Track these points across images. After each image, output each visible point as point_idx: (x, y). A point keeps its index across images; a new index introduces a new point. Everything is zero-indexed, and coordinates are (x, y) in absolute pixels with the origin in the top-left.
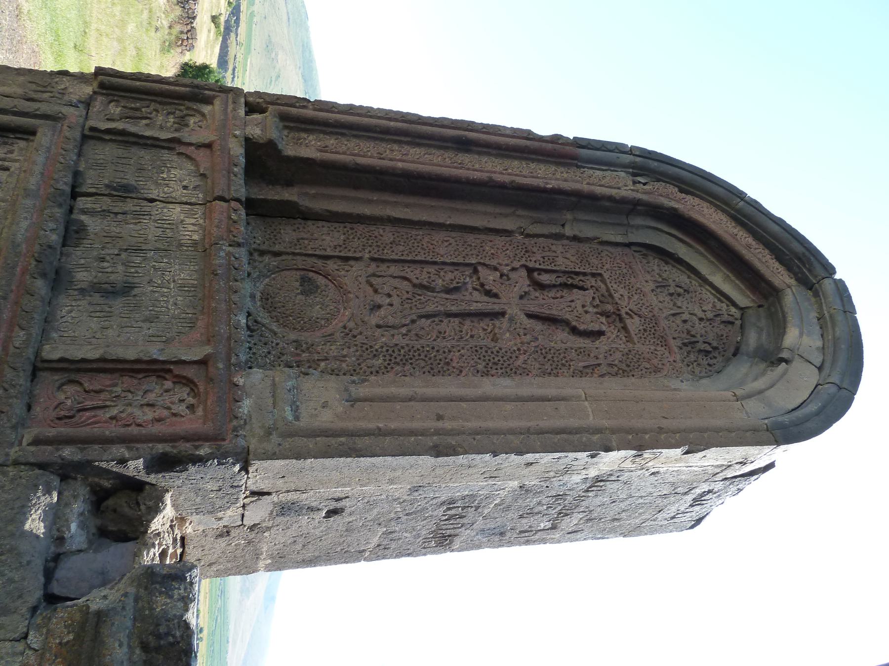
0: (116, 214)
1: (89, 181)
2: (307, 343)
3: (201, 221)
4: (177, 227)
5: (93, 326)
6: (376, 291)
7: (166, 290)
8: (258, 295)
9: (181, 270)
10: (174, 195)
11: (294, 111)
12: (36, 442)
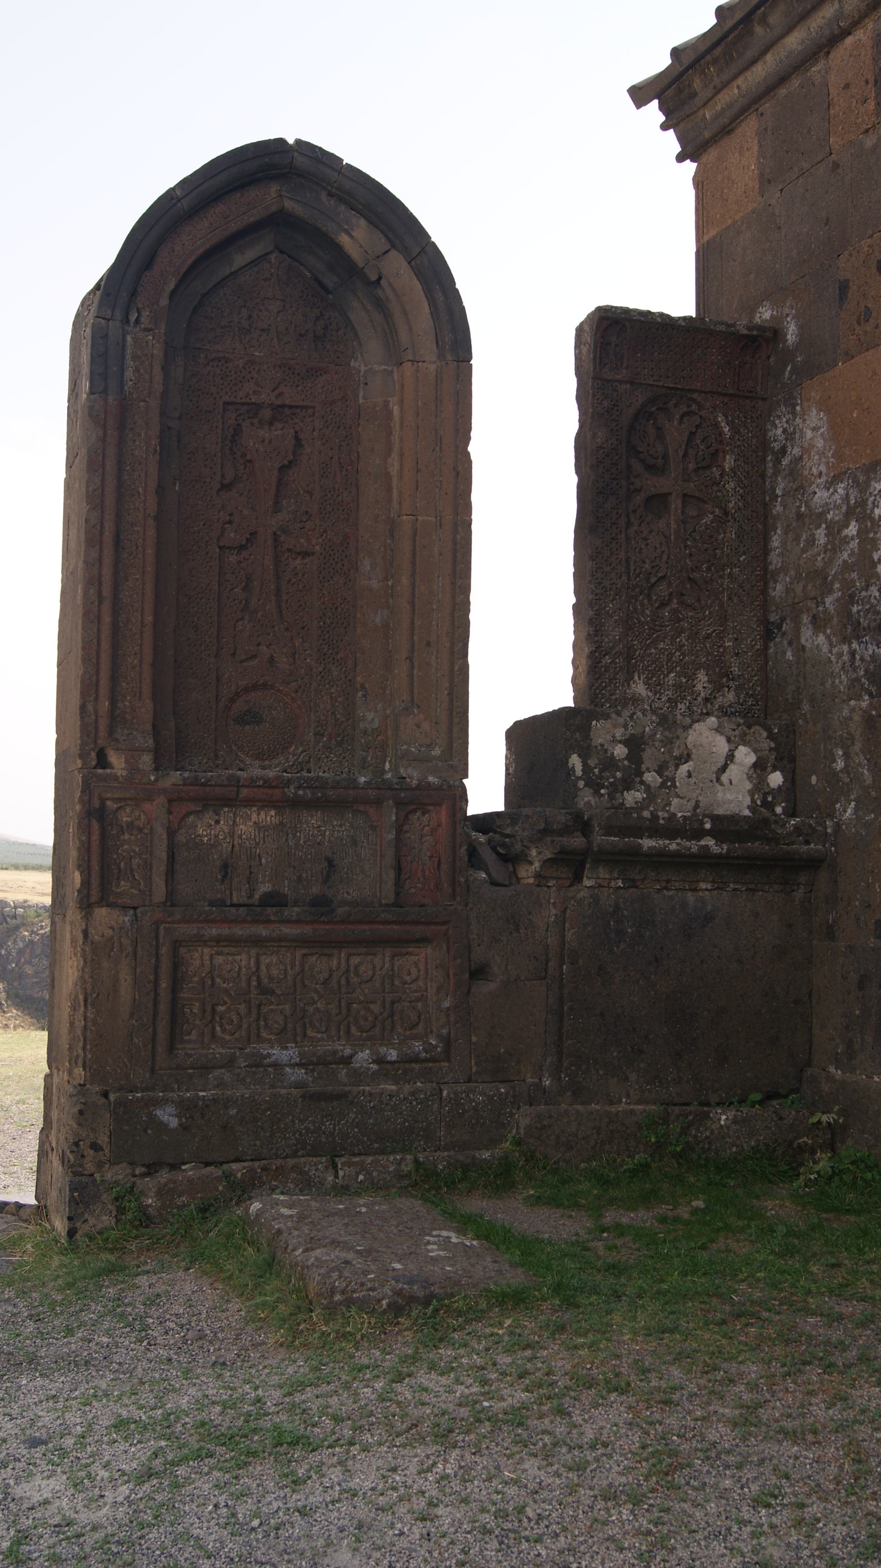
0: (251, 873)
1: (219, 896)
2: (317, 726)
3: (254, 809)
4: (263, 827)
5: (360, 878)
6: (254, 657)
7: (328, 833)
8: (257, 763)
9: (307, 823)
10: (227, 831)
11: (103, 724)
12: (454, 897)
